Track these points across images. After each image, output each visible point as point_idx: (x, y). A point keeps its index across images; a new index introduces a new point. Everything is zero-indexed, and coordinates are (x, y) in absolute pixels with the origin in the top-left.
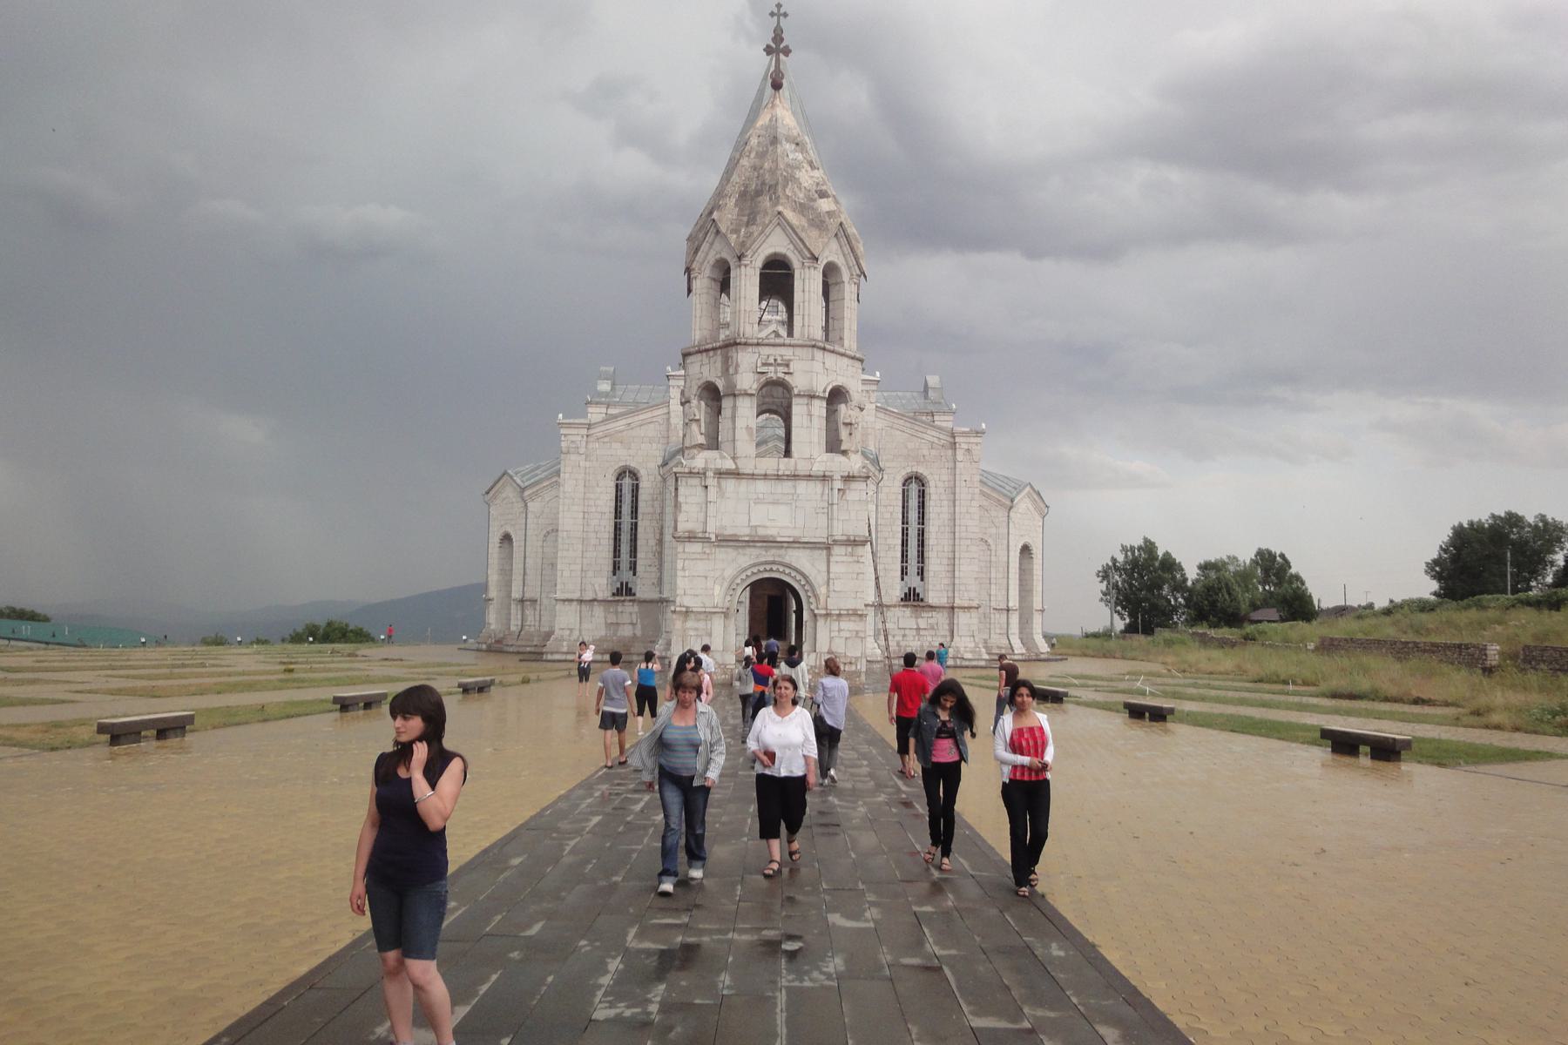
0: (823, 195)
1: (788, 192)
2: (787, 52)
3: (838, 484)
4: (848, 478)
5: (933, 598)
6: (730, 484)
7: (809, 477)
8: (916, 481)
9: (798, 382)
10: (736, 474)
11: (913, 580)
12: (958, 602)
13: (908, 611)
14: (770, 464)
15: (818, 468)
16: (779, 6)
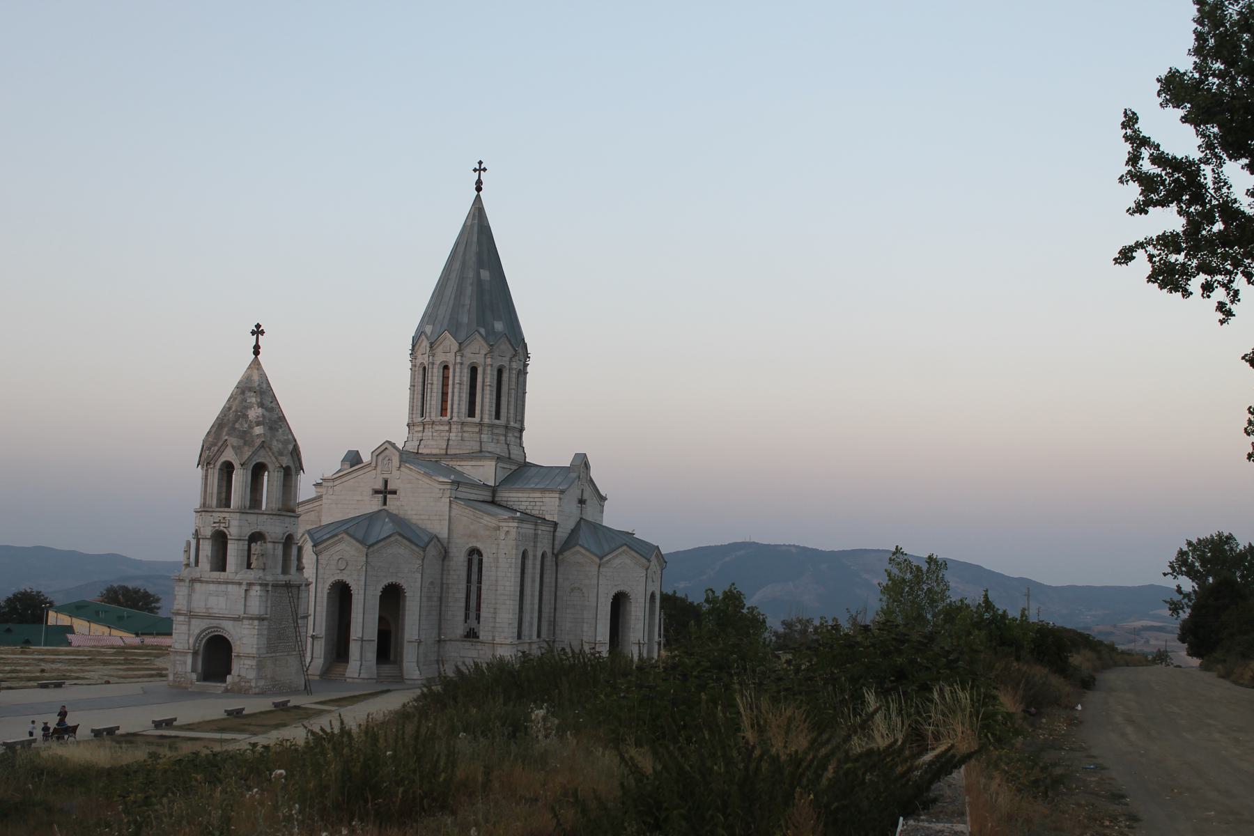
0: (258, 424)
1: (237, 426)
2: (262, 332)
3: (244, 587)
4: (250, 584)
5: (483, 636)
6: (197, 586)
7: (233, 583)
8: (474, 553)
9: (233, 531)
10: (201, 582)
11: (473, 623)
12: (498, 640)
13: (467, 645)
14: (216, 575)
15: (238, 578)
16: (480, 163)
